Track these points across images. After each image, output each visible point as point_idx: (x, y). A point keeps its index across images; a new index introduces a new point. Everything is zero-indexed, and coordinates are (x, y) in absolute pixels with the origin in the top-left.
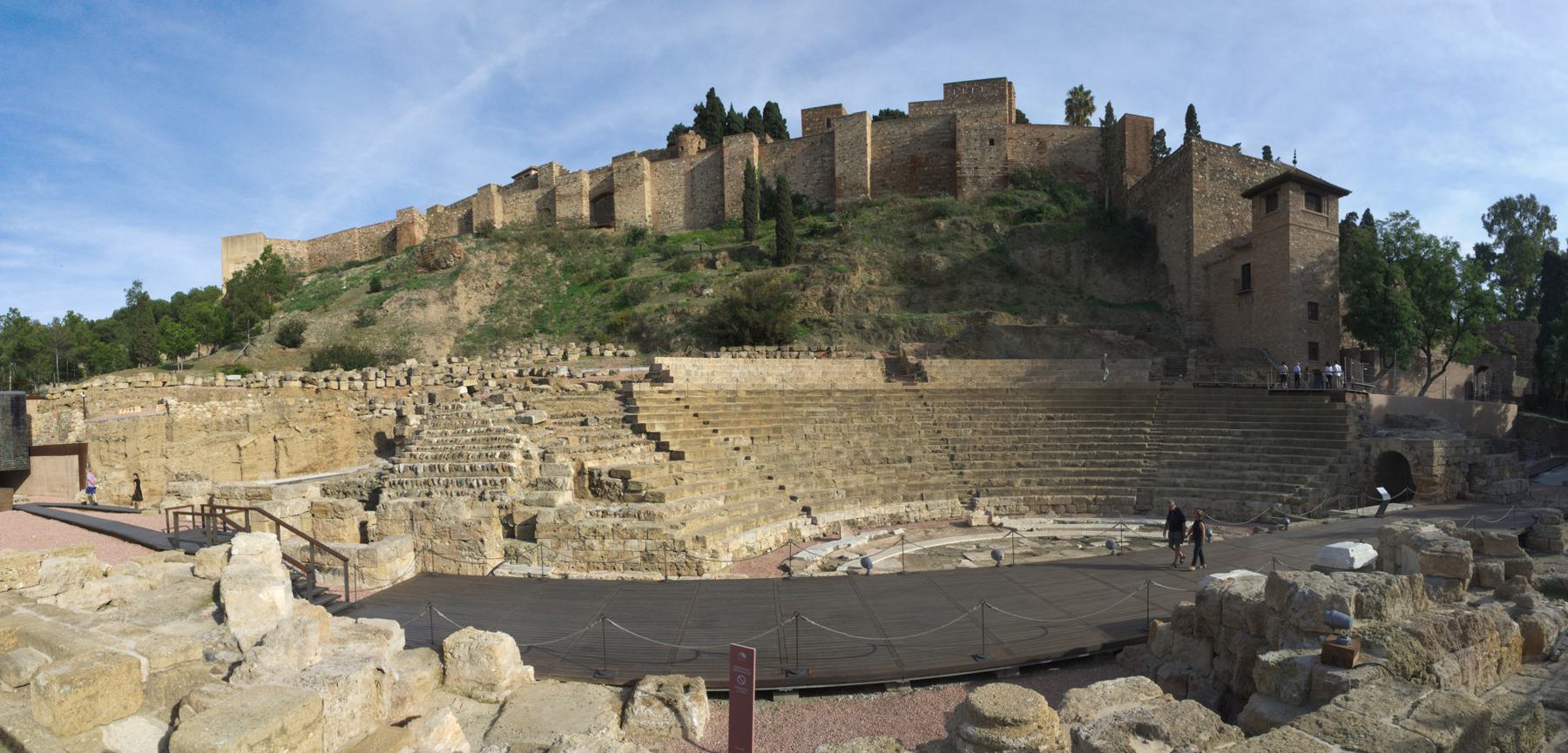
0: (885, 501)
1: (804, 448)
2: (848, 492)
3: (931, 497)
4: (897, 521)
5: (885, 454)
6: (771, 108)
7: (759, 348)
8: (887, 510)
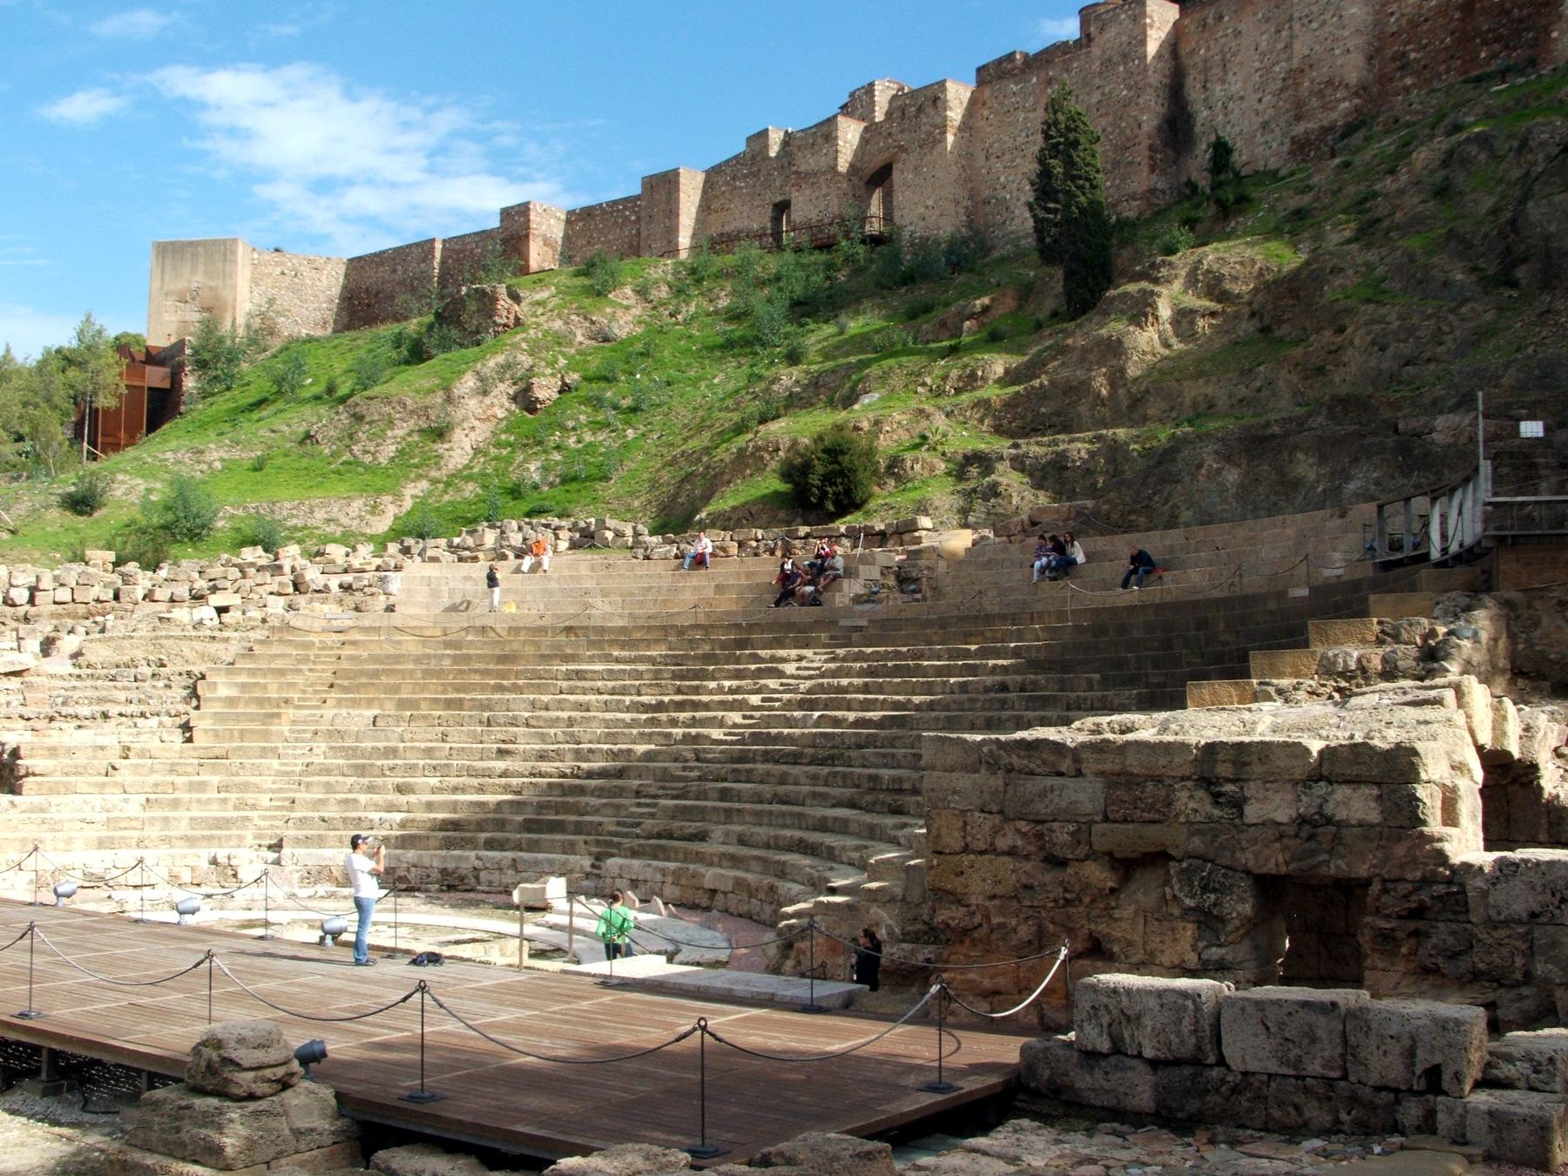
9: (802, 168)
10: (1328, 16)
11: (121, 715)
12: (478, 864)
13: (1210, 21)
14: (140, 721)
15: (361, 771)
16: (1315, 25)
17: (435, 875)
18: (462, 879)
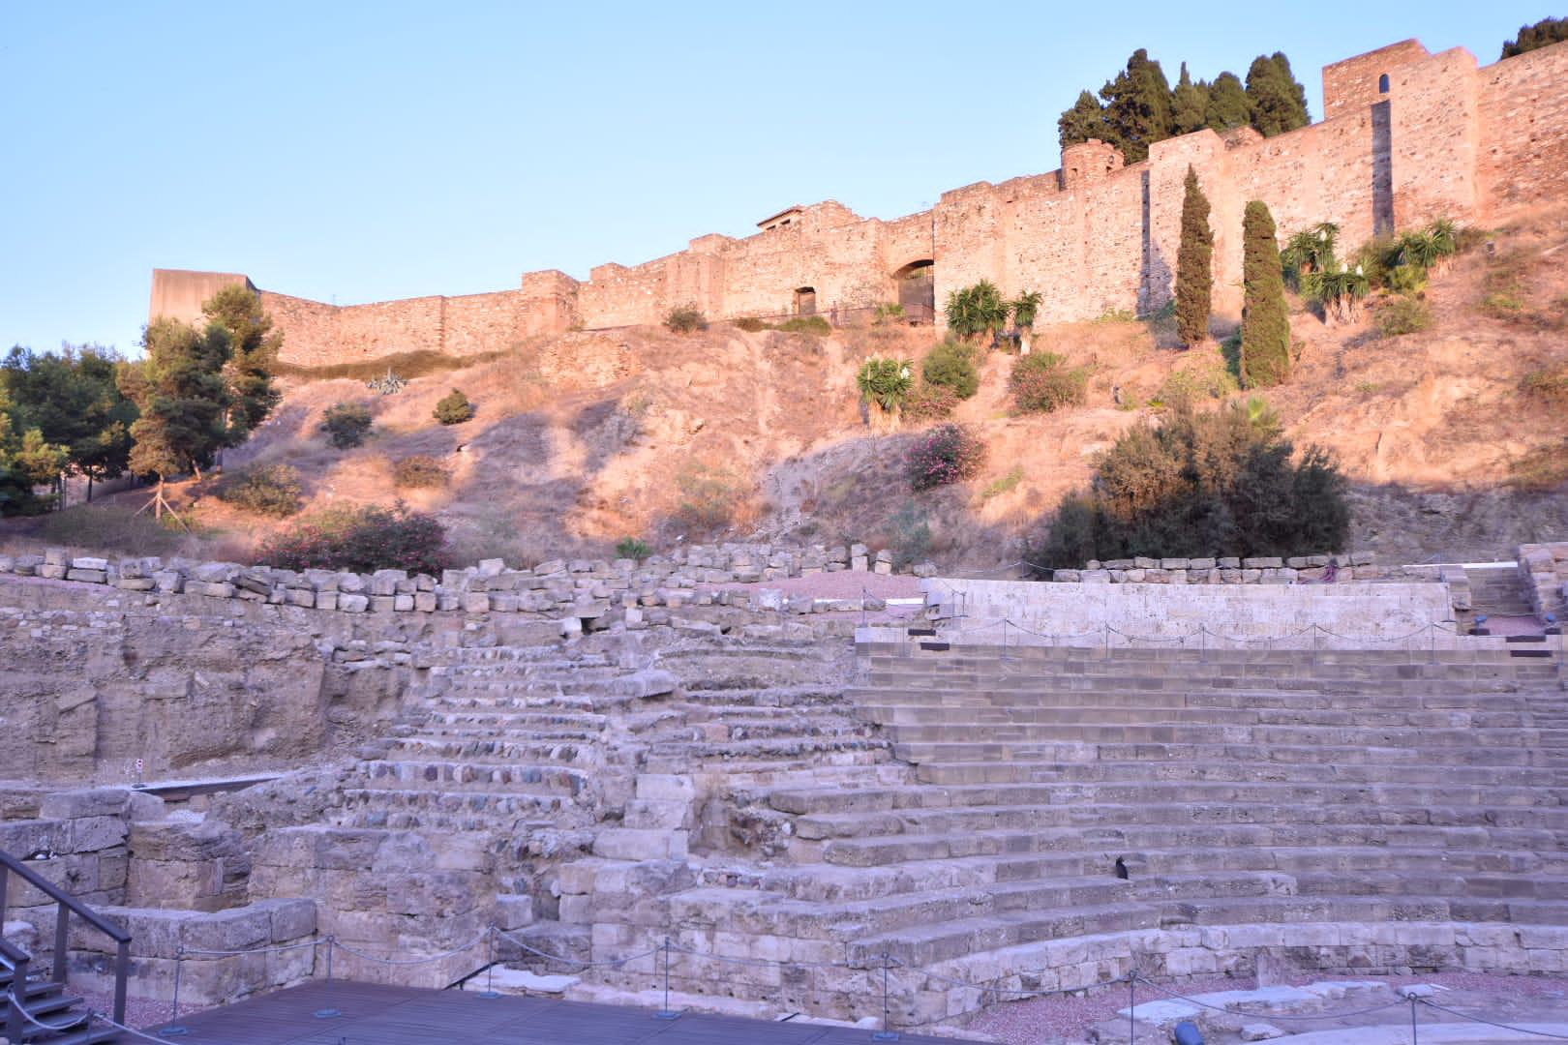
0: (1399, 914)
1: (1215, 777)
2: (1304, 888)
3: (1534, 917)
4: (1426, 962)
5: (1425, 802)
6: (1271, 69)
7: (1169, 563)
8: (1403, 935)
9: (837, 259)
10: (1434, 150)
11: (817, 749)
12: (1461, 939)
13: (1266, 155)
14: (834, 756)
15: (1164, 816)
16: (1417, 157)
17: (1402, 955)
18: (1440, 958)
